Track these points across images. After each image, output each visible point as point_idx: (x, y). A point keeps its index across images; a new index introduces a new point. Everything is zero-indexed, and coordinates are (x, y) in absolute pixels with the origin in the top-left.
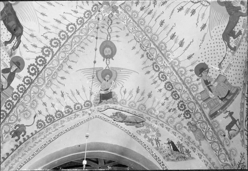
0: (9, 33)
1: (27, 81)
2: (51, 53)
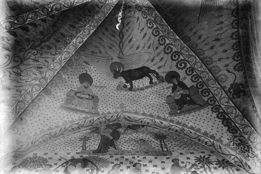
0: (144, 78)
1: (189, 72)
2: (170, 46)
